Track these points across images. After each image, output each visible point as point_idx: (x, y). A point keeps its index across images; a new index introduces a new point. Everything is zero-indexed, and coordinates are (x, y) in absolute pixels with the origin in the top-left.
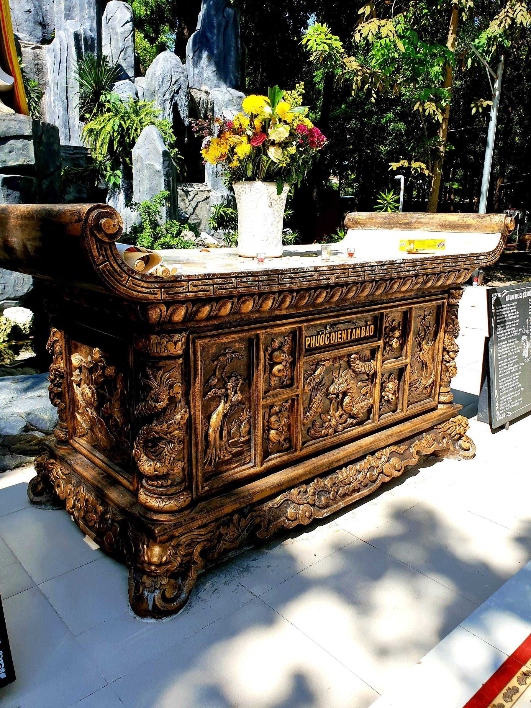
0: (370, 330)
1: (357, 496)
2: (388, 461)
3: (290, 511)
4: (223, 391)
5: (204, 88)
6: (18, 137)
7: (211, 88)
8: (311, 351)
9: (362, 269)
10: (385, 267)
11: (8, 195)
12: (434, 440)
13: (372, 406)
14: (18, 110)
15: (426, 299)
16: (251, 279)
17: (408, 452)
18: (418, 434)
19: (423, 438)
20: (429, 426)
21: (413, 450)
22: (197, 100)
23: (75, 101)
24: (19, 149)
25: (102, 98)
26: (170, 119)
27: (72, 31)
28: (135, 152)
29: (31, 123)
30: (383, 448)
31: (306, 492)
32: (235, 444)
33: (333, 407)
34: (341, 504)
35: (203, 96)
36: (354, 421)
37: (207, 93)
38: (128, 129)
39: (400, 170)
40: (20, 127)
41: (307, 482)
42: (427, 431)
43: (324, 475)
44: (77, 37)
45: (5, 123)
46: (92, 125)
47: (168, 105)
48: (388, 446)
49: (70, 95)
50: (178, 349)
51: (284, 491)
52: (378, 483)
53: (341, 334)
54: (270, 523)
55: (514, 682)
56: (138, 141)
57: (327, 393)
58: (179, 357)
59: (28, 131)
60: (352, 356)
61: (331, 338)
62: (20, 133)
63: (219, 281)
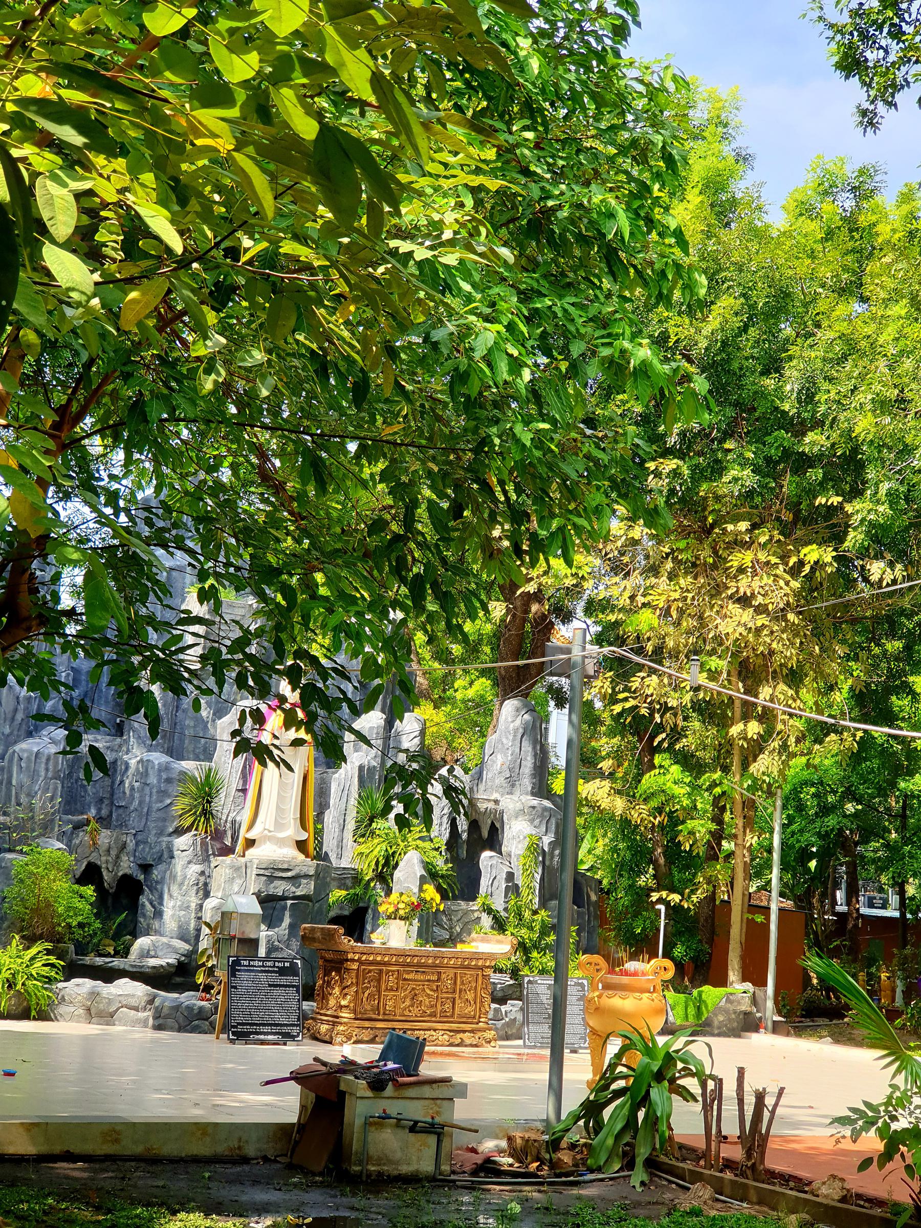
0: (435, 977)
7: (502, 795)
8: (405, 979)
14: (307, 856)
18: (464, 1032)
23: (351, 825)
25: (374, 825)
27: (357, 764)
28: (397, 874)
35: (491, 805)
37: (496, 802)
38: (394, 853)
39: (660, 900)
44: (361, 768)
46: (363, 849)
47: (445, 819)
49: (348, 819)
50: (355, 967)
56: (401, 864)
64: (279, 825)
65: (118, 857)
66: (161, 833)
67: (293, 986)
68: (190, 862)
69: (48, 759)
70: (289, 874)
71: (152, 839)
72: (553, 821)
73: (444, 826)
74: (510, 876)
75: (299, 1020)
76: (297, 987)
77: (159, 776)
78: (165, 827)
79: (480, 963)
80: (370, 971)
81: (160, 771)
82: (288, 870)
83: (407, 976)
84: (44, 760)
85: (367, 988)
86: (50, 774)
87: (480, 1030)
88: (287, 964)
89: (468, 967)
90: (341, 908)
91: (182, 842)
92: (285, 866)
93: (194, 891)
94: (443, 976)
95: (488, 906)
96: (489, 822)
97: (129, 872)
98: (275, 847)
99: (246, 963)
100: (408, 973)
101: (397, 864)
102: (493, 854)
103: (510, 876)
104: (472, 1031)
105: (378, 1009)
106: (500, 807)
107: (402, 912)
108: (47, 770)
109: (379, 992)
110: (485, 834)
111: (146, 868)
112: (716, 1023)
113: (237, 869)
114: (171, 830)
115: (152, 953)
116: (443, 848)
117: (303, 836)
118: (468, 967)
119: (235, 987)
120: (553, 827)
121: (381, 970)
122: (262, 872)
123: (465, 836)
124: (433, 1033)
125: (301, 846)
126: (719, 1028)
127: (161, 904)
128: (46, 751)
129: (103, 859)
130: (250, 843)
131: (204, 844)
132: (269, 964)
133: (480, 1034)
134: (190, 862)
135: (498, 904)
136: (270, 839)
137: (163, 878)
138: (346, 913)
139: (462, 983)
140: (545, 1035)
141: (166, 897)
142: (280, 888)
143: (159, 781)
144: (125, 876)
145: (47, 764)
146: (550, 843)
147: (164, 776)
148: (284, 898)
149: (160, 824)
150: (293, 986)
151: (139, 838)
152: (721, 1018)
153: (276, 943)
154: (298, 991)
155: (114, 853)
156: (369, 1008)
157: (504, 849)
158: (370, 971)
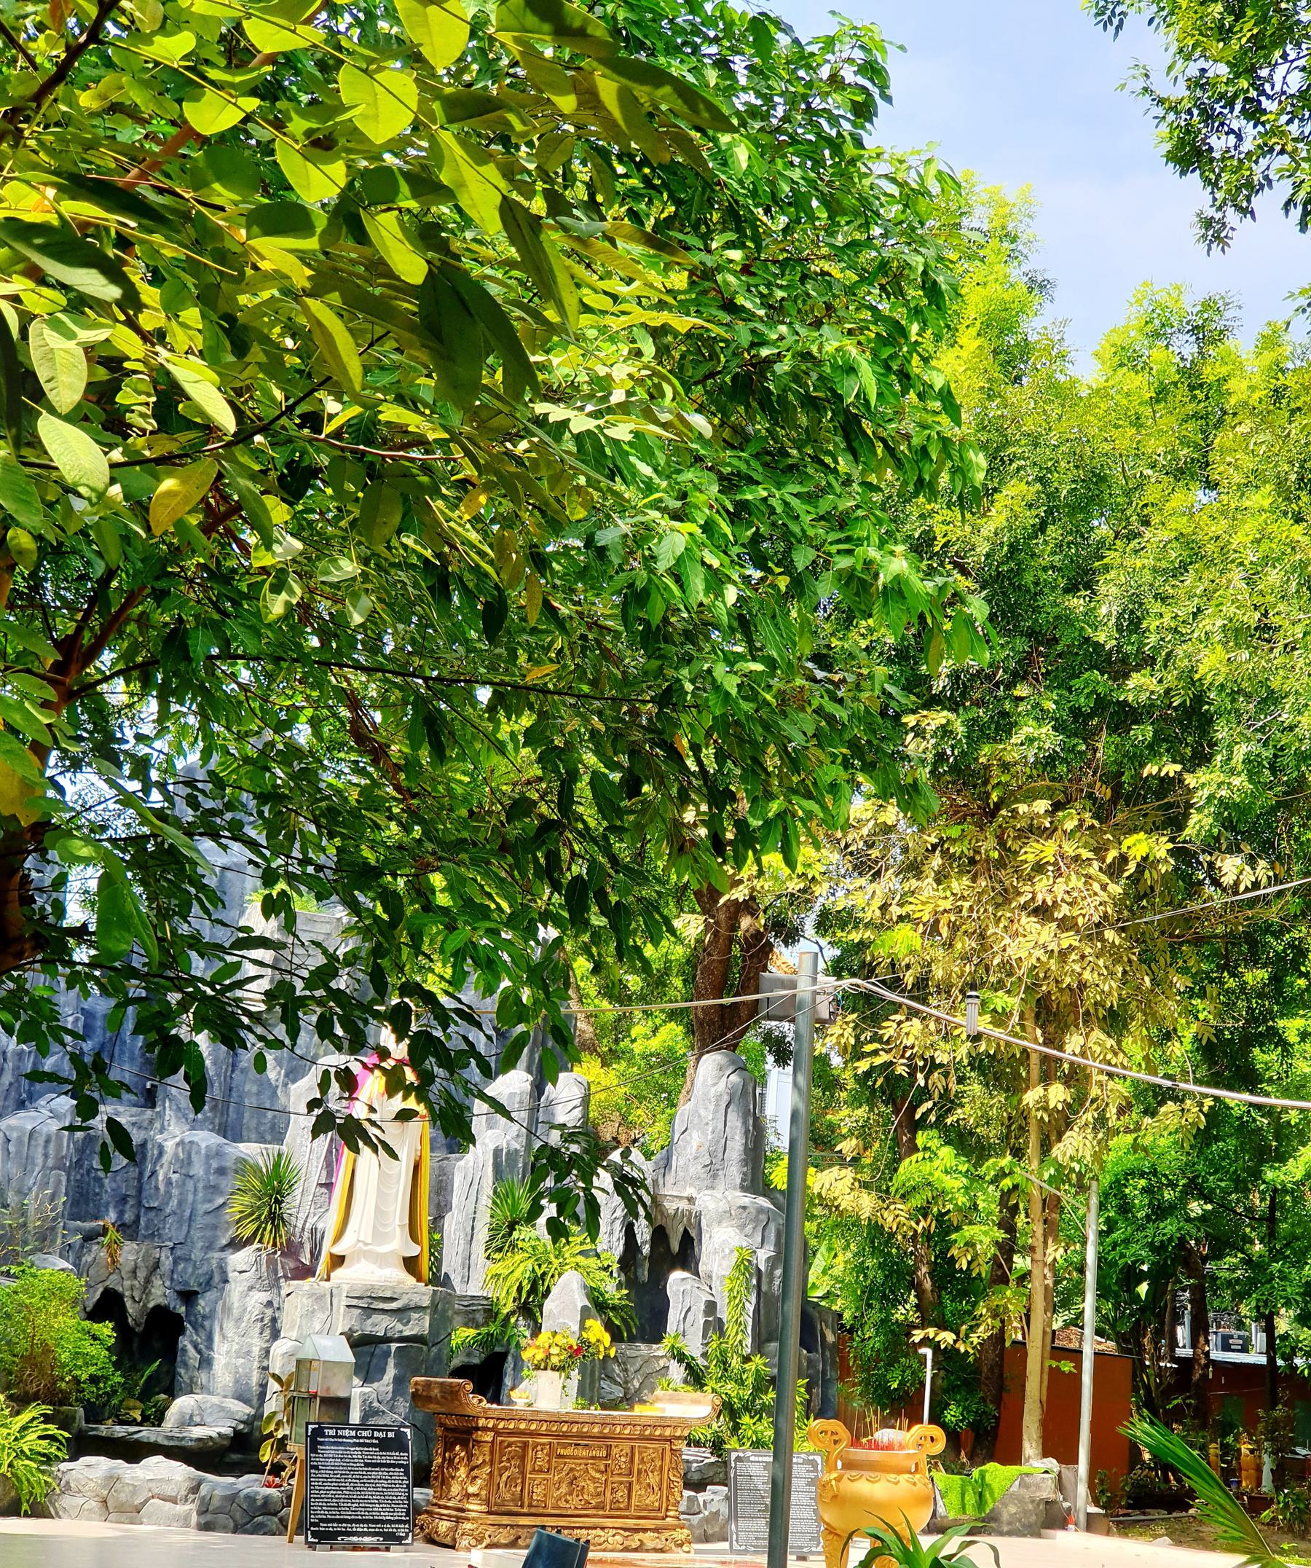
0: (604, 1453)
5: (689, 1191)
7: (699, 1190)
8: (560, 1456)
14: (419, 1280)
18: (645, 1530)
22: (671, 1212)
23: (482, 1235)
26: (619, 1249)
27: (492, 1147)
28: (549, 1305)
35: (683, 1205)
37: (691, 1200)
38: (544, 1274)
39: (926, 1341)
44: (497, 1152)
46: (500, 1268)
47: (618, 1226)
49: (478, 1225)
50: (489, 1439)
56: (554, 1290)
64: (379, 1236)
65: (148, 1280)
66: (209, 1247)
68: (251, 1288)
69: (48, 1141)
70: (394, 1305)
71: (196, 1255)
72: (772, 1227)
73: (616, 1235)
74: (711, 1307)
75: (408, 1514)
77: (208, 1165)
78: (215, 1238)
79: (668, 1432)
80: (509, 1445)
81: (208, 1157)
82: (392, 1299)
83: (562, 1452)
84: (41, 1141)
85: (506, 1469)
86: (50, 1163)
87: (666, 1528)
88: (391, 1435)
89: (650, 1439)
90: (469, 1355)
91: (240, 1259)
93: (257, 1330)
94: (614, 1451)
95: (679, 1350)
96: (681, 1229)
98: (374, 1267)
99: (332, 1432)
100: (565, 1446)
101: (548, 1291)
102: (686, 1274)
103: (711, 1307)
104: (656, 1530)
105: (521, 1499)
106: (696, 1208)
107: (555, 1360)
108: (46, 1156)
109: (523, 1473)
110: (675, 1246)
111: (189, 1297)
112: (1005, 1517)
113: (320, 1298)
114: (224, 1242)
115: (197, 1419)
116: (615, 1267)
117: (414, 1250)
118: (650, 1439)
119: (316, 1468)
120: (773, 1236)
121: (526, 1443)
122: (354, 1302)
123: (646, 1250)
124: (599, 1532)
125: (411, 1264)
126: (1009, 1523)
127: (210, 1347)
128: (45, 1129)
129: (127, 1283)
130: (338, 1261)
131: (271, 1262)
132: (365, 1434)
133: (667, 1534)
134: (251, 1288)
135: (693, 1347)
137: (213, 1311)
138: (476, 1361)
139: (642, 1461)
140: (760, 1535)
141: (217, 1338)
142: (379, 1325)
143: (207, 1172)
144: (158, 1308)
145: (46, 1147)
146: (768, 1259)
147: (215, 1165)
148: (386, 1340)
149: (209, 1233)
151: (179, 1253)
152: (1012, 1509)
153: (376, 1404)
154: (406, 1473)
155: (142, 1274)
156: (508, 1496)
157: (701, 1268)
158: (509, 1445)
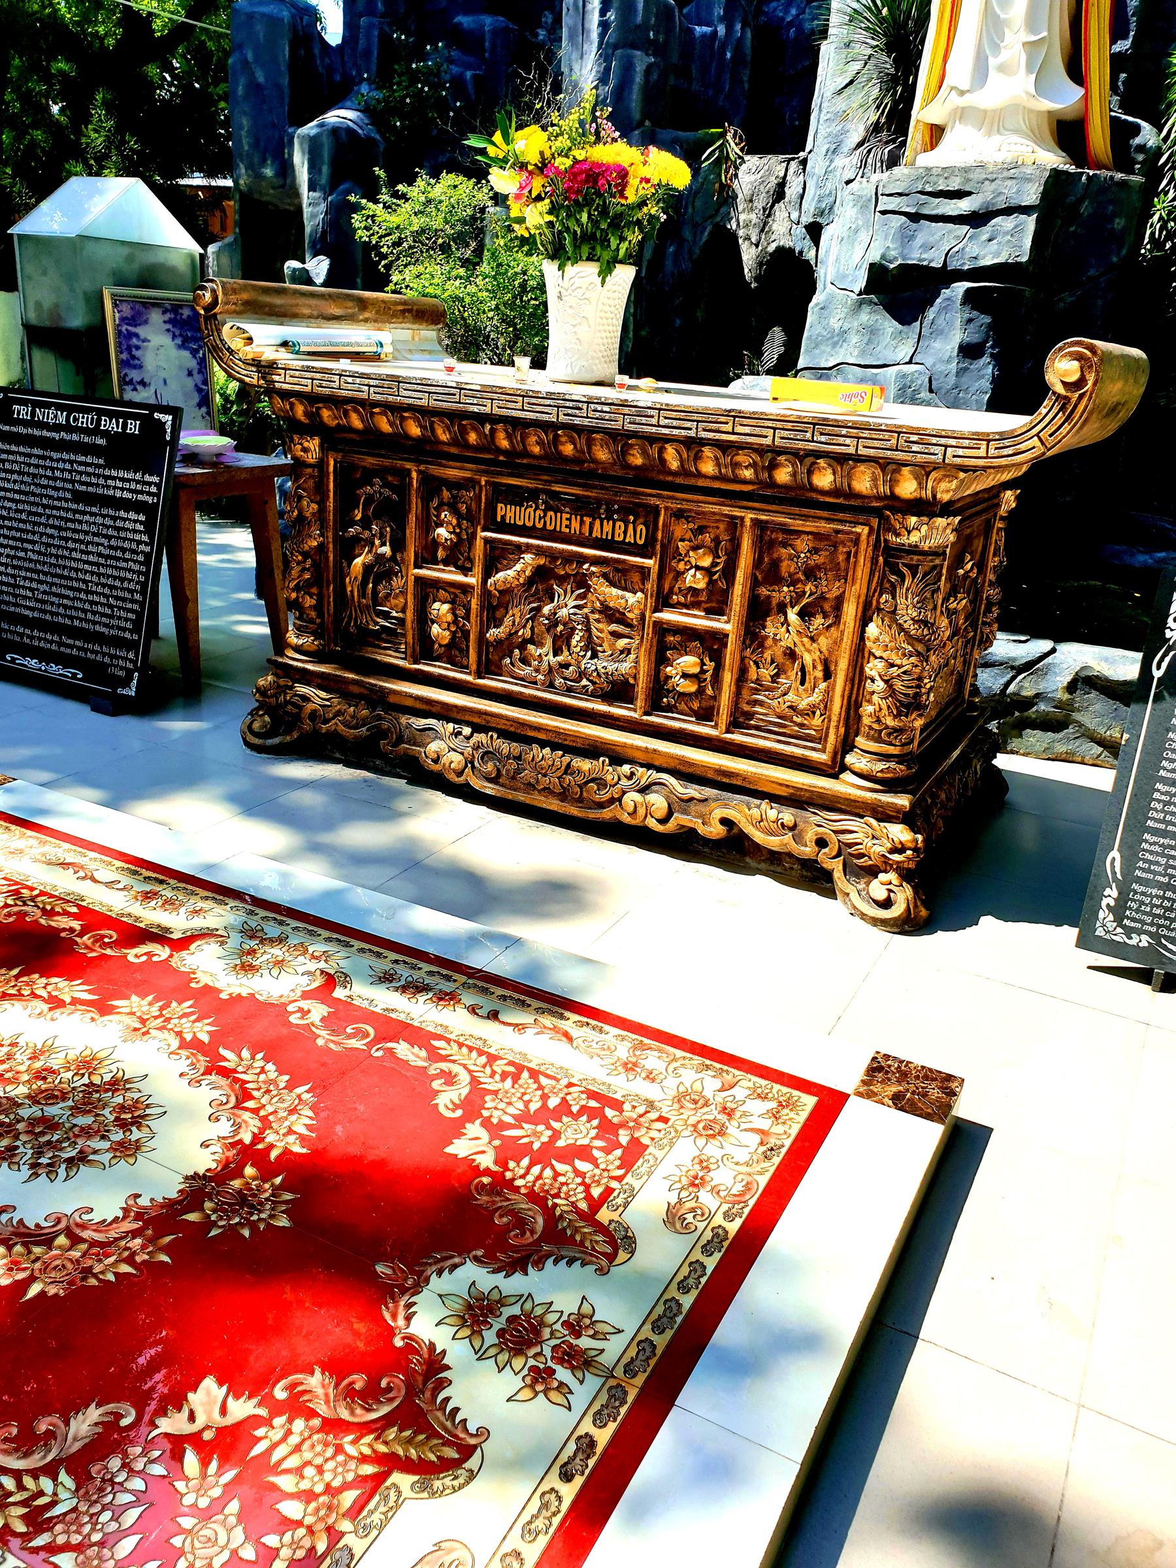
1: (554, 805)
2: (643, 790)
3: (434, 747)
4: (367, 534)
6: (1008, 211)
9: (548, 402)
10: (606, 408)
11: (970, 321)
12: (793, 828)
13: (635, 677)
15: (796, 510)
16: (358, 380)
17: (701, 808)
19: (758, 807)
20: (783, 792)
21: (719, 813)
24: (1006, 233)
29: (1043, 181)
30: (642, 765)
31: (468, 738)
32: (386, 616)
33: (549, 642)
34: (521, 797)
36: (591, 688)
40: (1018, 191)
41: (477, 729)
42: (774, 798)
43: (504, 734)
45: (994, 186)
48: (659, 770)
51: (439, 717)
52: (606, 814)
53: (569, 519)
54: (400, 739)
55: (661, 1341)
57: (538, 609)
58: (311, 466)
59: (1031, 195)
60: (586, 566)
61: (548, 519)
62: (1014, 202)
63: (318, 376)
67: (139, 507)
75: (137, 625)
76: (148, 510)
79: (864, 482)
82: (959, 194)
88: (133, 427)
92: (954, 185)
97: (787, 242)
100: (517, 497)
104: (798, 800)
111: (814, 231)
117: (1068, 97)
118: (800, 497)
132: (84, 420)
136: (962, 114)
139: (768, 573)
142: (935, 246)
144: (780, 250)
145: (603, 12)
150: (139, 507)
154: (149, 528)
155: (760, 204)
